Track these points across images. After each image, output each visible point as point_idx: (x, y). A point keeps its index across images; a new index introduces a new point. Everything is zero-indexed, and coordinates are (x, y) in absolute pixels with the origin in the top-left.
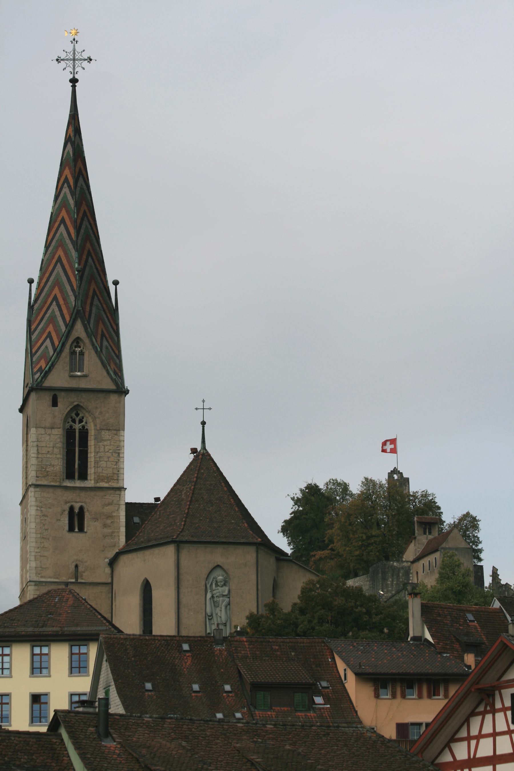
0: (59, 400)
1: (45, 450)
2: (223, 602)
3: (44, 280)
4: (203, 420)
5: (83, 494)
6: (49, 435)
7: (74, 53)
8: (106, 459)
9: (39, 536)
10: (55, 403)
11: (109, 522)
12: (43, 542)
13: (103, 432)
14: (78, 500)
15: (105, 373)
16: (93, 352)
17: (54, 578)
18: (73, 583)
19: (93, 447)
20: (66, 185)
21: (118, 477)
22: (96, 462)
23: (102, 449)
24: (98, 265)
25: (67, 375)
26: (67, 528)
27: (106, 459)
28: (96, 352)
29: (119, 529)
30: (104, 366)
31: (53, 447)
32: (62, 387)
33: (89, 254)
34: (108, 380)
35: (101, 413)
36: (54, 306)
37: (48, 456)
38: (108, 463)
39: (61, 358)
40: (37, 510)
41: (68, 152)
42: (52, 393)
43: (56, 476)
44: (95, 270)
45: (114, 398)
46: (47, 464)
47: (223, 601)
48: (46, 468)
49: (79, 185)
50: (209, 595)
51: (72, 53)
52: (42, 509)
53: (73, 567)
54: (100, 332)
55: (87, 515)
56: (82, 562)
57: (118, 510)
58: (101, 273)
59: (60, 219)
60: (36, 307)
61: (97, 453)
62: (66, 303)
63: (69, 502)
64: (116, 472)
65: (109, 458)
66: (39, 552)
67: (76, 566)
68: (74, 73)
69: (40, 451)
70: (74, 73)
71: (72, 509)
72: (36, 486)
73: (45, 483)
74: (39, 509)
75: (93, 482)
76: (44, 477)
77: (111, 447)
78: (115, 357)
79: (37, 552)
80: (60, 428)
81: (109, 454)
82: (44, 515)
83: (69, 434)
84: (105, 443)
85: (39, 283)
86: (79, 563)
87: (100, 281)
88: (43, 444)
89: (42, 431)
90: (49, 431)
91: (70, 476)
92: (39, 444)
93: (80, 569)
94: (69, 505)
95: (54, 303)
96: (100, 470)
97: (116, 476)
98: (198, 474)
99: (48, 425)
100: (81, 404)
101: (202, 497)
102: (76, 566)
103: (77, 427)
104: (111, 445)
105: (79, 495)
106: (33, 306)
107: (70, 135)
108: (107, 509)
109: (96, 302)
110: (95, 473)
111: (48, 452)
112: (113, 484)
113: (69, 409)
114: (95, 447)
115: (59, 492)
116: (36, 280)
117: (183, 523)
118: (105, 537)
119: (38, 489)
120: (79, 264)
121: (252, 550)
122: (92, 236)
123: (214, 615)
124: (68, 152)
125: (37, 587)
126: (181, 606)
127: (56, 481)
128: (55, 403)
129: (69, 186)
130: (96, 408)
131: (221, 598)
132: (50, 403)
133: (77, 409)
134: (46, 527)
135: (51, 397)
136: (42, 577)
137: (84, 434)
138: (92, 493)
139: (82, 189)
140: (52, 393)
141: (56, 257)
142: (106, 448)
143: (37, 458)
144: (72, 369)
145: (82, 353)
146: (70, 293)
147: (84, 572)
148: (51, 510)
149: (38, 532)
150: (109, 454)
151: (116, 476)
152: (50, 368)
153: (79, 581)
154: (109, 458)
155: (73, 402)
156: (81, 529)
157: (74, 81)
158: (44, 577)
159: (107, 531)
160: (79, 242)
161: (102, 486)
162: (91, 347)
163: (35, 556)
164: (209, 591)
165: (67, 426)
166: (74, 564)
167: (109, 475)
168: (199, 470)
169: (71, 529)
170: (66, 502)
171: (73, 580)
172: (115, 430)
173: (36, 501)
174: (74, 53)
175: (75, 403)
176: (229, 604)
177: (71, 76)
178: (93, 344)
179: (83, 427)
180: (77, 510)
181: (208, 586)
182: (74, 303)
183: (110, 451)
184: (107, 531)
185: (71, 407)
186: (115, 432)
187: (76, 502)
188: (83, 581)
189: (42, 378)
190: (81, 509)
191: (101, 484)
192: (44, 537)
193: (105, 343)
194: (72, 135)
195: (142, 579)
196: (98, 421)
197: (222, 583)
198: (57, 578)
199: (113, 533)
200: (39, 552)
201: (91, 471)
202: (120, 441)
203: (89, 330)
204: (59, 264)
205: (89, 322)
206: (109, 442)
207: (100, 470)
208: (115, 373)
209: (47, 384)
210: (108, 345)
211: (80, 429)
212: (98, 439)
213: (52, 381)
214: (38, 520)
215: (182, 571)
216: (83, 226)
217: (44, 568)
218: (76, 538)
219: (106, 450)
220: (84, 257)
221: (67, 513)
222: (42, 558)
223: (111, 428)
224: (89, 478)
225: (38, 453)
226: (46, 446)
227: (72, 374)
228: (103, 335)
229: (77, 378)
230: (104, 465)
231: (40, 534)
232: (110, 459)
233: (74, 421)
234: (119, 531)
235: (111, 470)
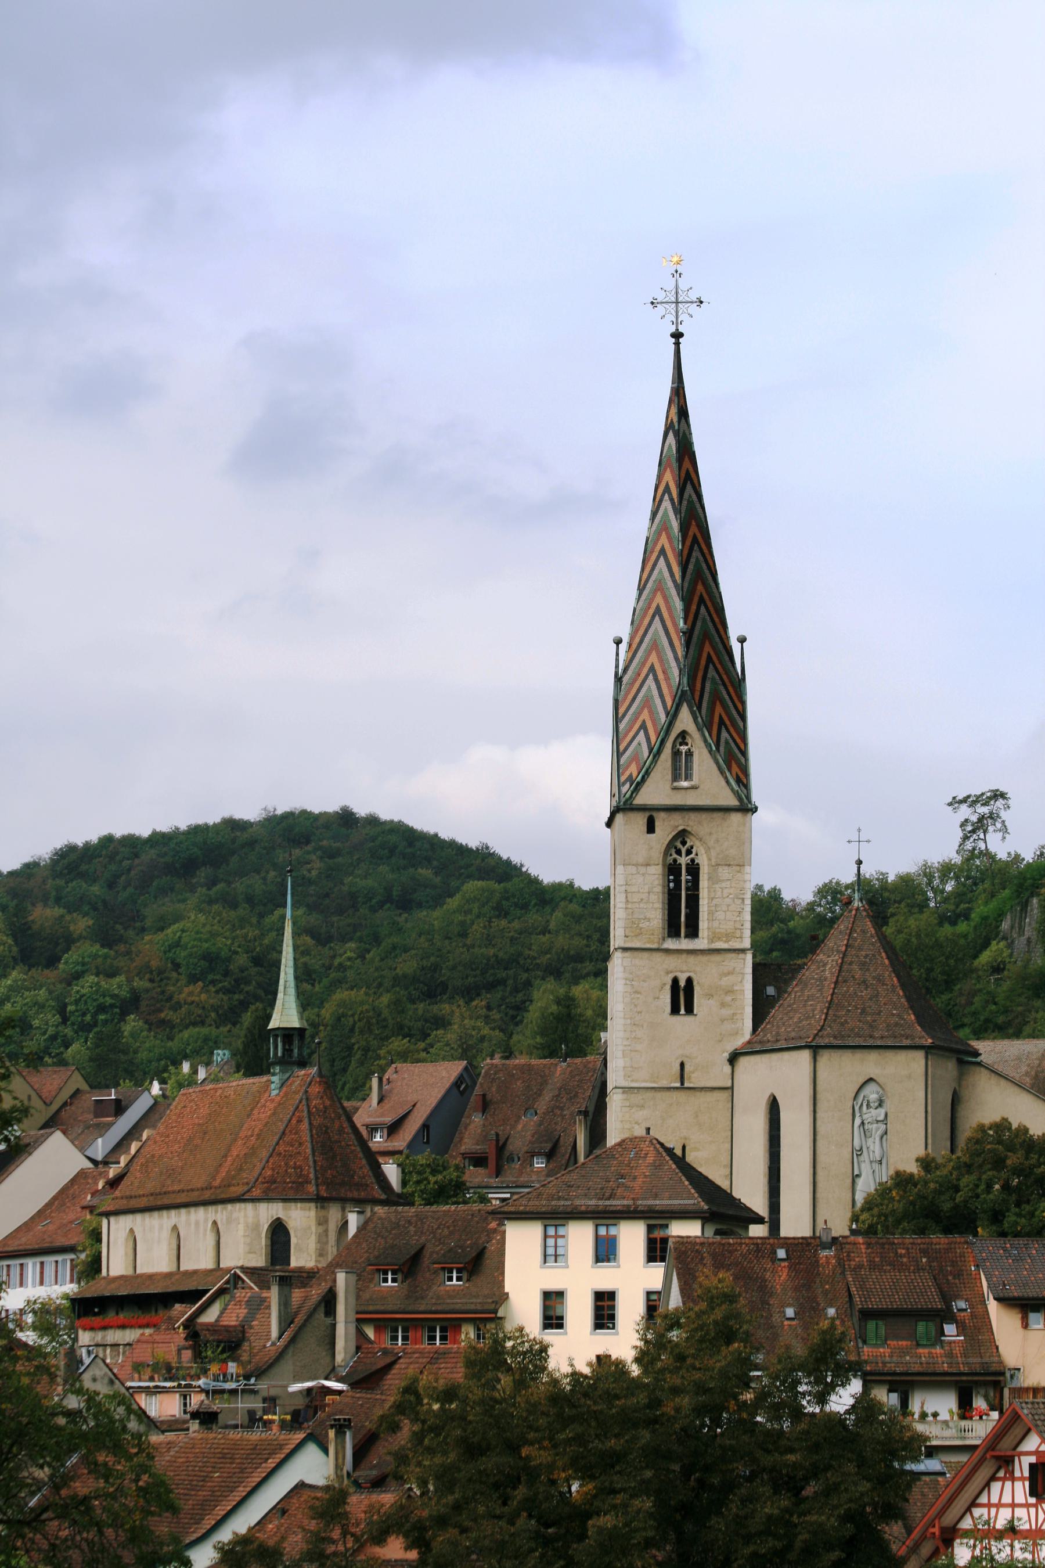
0: (657, 824)
1: (636, 898)
2: (877, 1130)
3: (637, 640)
5: (691, 959)
6: (643, 875)
7: (677, 293)
8: (725, 908)
9: (629, 1021)
10: (651, 828)
11: (728, 998)
13: (720, 869)
14: (685, 968)
15: (723, 782)
16: (705, 751)
18: (677, 1088)
20: (666, 497)
22: (711, 913)
23: (719, 894)
24: (715, 616)
25: (668, 786)
26: (668, 1009)
27: (725, 908)
28: (710, 751)
29: (744, 1008)
30: (722, 773)
33: (701, 600)
35: (717, 841)
37: (642, 905)
39: (659, 762)
41: (670, 446)
42: (647, 814)
44: (710, 624)
45: (736, 818)
46: (642, 917)
49: (686, 496)
50: (858, 1121)
51: (673, 292)
54: (716, 719)
58: (720, 627)
59: (658, 548)
60: (625, 680)
61: (712, 899)
62: (667, 679)
64: (738, 926)
65: (728, 906)
67: (682, 1065)
68: (677, 322)
69: (630, 899)
70: (677, 322)
71: (675, 981)
72: (625, 949)
75: (706, 941)
76: (636, 936)
77: (732, 891)
78: (740, 755)
82: (637, 992)
83: (673, 870)
84: (724, 885)
85: (630, 645)
87: (718, 640)
88: (634, 889)
89: (632, 869)
90: (642, 870)
91: (673, 930)
92: (629, 889)
93: (687, 1068)
94: (671, 976)
95: (651, 677)
96: (716, 924)
97: (738, 931)
99: (641, 860)
100: (689, 829)
101: (853, 977)
102: (682, 1065)
103: (683, 860)
106: (621, 677)
107: (672, 420)
108: (725, 981)
109: (712, 672)
110: (708, 928)
113: (671, 836)
114: (709, 891)
115: (658, 957)
116: (626, 640)
117: (823, 1017)
118: (722, 1021)
120: (685, 623)
121: (920, 1055)
122: (707, 572)
123: (864, 1149)
124: (670, 446)
126: (818, 1138)
127: (652, 942)
128: (651, 828)
129: (672, 500)
130: (711, 834)
131: (875, 1126)
133: (682, 835)
135: (645, 820)
136: (632, 1081)
137: (694, 870)
138: (704, 959)
139: (690, 502)
140: (647, 814)
141: (654, 606)
142: (725, 891)
144: (676, 777)
145: (689, 754)
146: (673, 664)
147: (693, 1072)
151: (738, 931)
152: (643, 777)
153: (686, 1085)
154: (728, 906)
156: (689, 1010)
157: (677, 336)
158: (636, 1081)
159: (726, 1012)
160: (686, 585)
162: (702, 744)
164: (857, 1114)
165: (670, 860)
168: (850, 933)
169: (675, 1010)
170: (668, 973)
171: (678, 1085)
174: (677, 293)
175: (681, 828)
176: (886, 1133)
177: (673, 329)
178: (705, 741)
179: (693, 860)
180: (682, 983)
181: (857, 1108)
182: (677, 680)
184: (726, 1012)
185: (674, 834)
186: (738, 868)
187: (682, 972)
188: (691, 1085)
189: (632, 793)
190: (689, 981)
193: (724, 734)
194: (675, 420)
196: (713, 853)
197: (876, 1104)
198: (654, 1082)
199: (734, 1014)
201: (703, 925)
202: (745, 881)
203: (699, 719)
204: (657, 618)
205: (699, 708)
207: (716, 924)
208: (738, 781)
209: (640, 800)
210: (729, 738)
211: (687, 864)
212: (713, 879)
213: (647, 796)
215: (819, 1088)
216: (693, 560)
218: (682, 1020)
220: (694, 607)
221: (668, 988)
224: (700, 934)
225: (627, 901)
227: (676, 784)
228: (722, 722)
229: (683, 791)
232: (730, 908)
235: (732, 923)
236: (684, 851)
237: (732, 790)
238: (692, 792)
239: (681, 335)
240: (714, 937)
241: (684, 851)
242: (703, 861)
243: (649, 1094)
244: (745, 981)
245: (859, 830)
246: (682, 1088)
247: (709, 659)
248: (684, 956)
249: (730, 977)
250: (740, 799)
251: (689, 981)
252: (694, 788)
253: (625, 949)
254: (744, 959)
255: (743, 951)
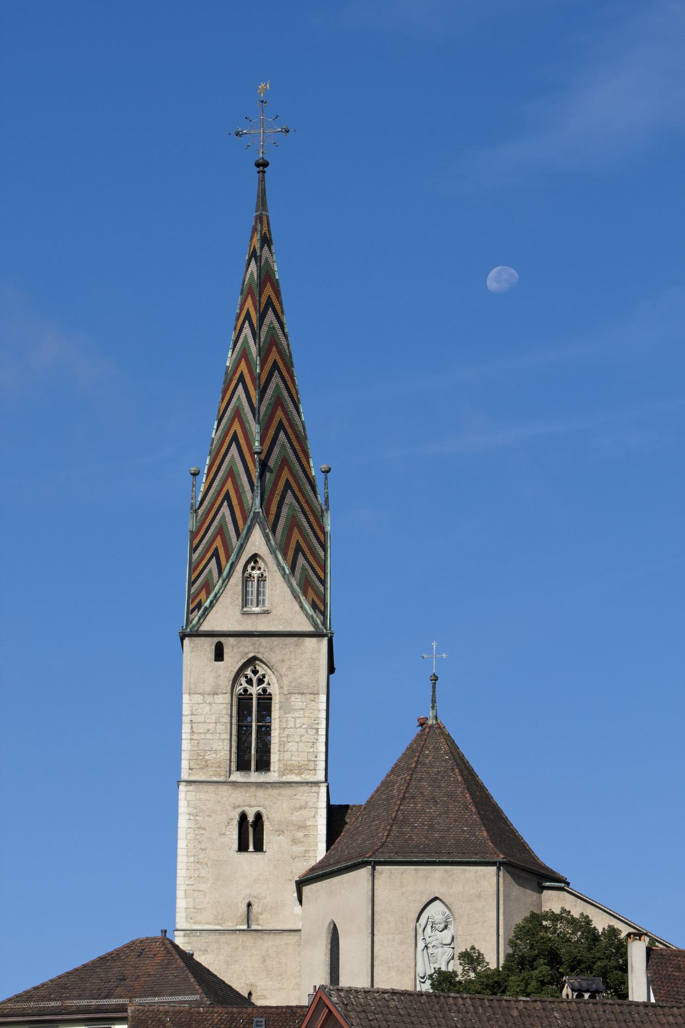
0: (226, 650)
1: (201, 728)
5: (260, 793)
6: (210, 704)
8: (297, 739)
9: (192, 859)
10: (219, 655)
11: (300, 835)
12: (198, 869)
13: (293, 698)
14: (253, 803)
15: (297, 607)
16: (278, 575)
17: (215, 924)
18: (243, 930)
19: (277, 721)
20: (247, 324)
21: (315, 765)
22: (282, 744)
23: (291, 724)
24: (295, 444)
26: (235, 846)
27: (297, 739)
28: (284, 575)
30: (296, 597)
31: (216, 723)
32: (231, 631)
33: (281, 426)
34: (302, 617)
35: (290, 668)
36: (225, 509)
37: (208, 736)
38: (300, 744)
39: (228, 587)
40: (190, 819)
41: (252, 273)
42: (216, 640)
43: (219, 767)
44: (290, 451)
47: (443, 954)
48: (204, 756)
49: (267, 321)
50: (421, 944)
52: (197, 818)
53: (245, 907)
54: (293, 545)
55: (267, 826)
56: (258, 898)
57: (314, 817)
58: (301, 455)
59: (237, 375)
61: (284, 729)
63: (239, 807)
65: (301, 736)
66: (192, 885)
69: (194, 730)
71: (243, 817)
73: (203, 778)
74: (192, 817)
75: (276, 774)
76: (201, 769)
77: (305, 720)
78: (318, 583)
79: (188, 885)
80: (226, 693)
81: (302, 731)
82: (199, 828)
83: (243, 703)
84: (296, 714)
86: (253, 901)
87: (298, 467)
88: (200, 719)
89: (199, 698)
90: (209, 699)
91: (243, 765)
92: (195, 719)
93: (255, 909)
94: (239, 811)
95: (225, 503)
96: (287, 756)
97: (312, 763)
98: (419, 757)
99: (208, 689)
100: (260, 656)
101: (422, 793)
102: (249, 905)
103: (254, 690)
104: (305, 717)
105: (255, 796)
108: (297, 816)
109: (289, 498)
110: (279, 760)
111: (208, 730)
112: (307, 777)
113: (240, 664)
114: (280, 721)
115: (224, 790)
117: (386, 833)
118: (294, 858)
119: (191, 788)
120: (262, 443)
122: (288, 400)
124: (252, 273)
125: (187, 938)
127: (220, 776)
128: (219, 655)
129: (251, 325)
130: (283, 661)
131: (440, 950)
132: (212, 655)
134: (203, 846)
135: (213, 647)
136: (195, 923)
137: (265, 701)
138: (275, 792)
142: (298, 721)
143: (191, 739)
144: (245, 603)
145: (262, 579)
147: (261, 914)
148: (211, 819)
149: (189, 854)
150: (302, 731)
152: (211, 602)
153: (254, 927)
154: (301, 736)
155: (248, 653)
156: (259, 847)
158: (199, 923)
160: (263, 409)
161: (291, 780)
162: (276, 568)
163: (186, 890)
164: (420, 937)
165: (239, 689)
166: (246, 902)
167: (301, 763)
169: (243, 847)
170: (235, 808)
171: (245, 927)
172: (311, 694)
173: (188, 806)
175: (251, 655)
178: (279, 564)
179: (265, 690)
180: (251, 818)
181: (420, 930)
182: (250, 502)
183: (304, 726)
185: (243, 661)
186: (312, 697)
187: (250, 806)
188: (259, 928)
189: (200, 619)
190: (259, 817)
191: (289, 776)
192: (201, 861)
193: (301, 561)
194: (258, 246)
195: (328, 921)
196: (286, 681)
197: (442, 926)
198: (219, 924)
200: (192, 885)
201: (274, 758)
203: (272, 542)
204: (234, 445)
205: (274, 530)
206: (302, 712)
207: (287, 756)
208: (314, 606)
210: (307, 565)
212: (286, 708)
214: (191, 836)
217: (198, 909)
219: (298, 725)
220: (271, 432)
222: (196, 894)
223: (305, 691)
224: (272, 769)
226: (205, 722)
227: (245, 609)
228: (298, 549)
229: (254, 616)
230: (295, 748)
231: (194, 856)
232: (303, 739)
233: (250, 682)
234: (316, 849)
236: (255, 679)
237: (307, 615)
238: (263, 618)
239: (265, 164)
240: (287, 769)
241: (255, 679)
242: (274, 690)
243: (213, 937)
244: (318, 816)
246: (249, 930)
247: (288, 486)
248: (253, 789)
249: (303, 812)
250: (315, 624)
251: (259, 816)
252: (266, 612)
253: (189, 782)
254: (318, 793)
255: (317, 784)
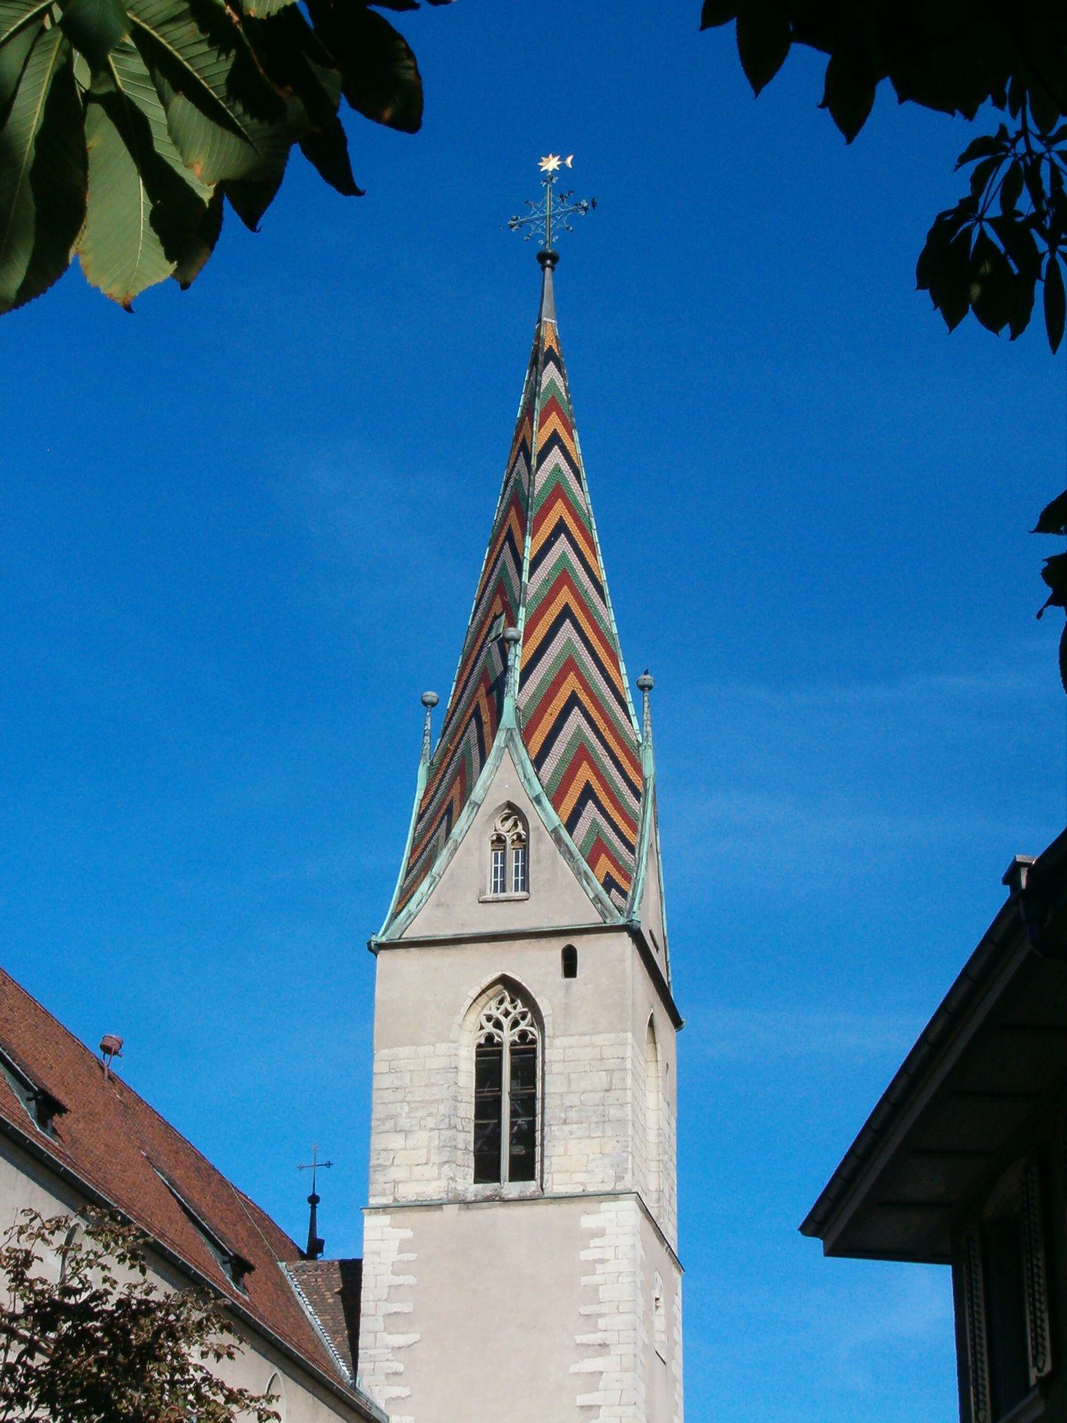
4: (314, 1194)
245: (329, 1165)
